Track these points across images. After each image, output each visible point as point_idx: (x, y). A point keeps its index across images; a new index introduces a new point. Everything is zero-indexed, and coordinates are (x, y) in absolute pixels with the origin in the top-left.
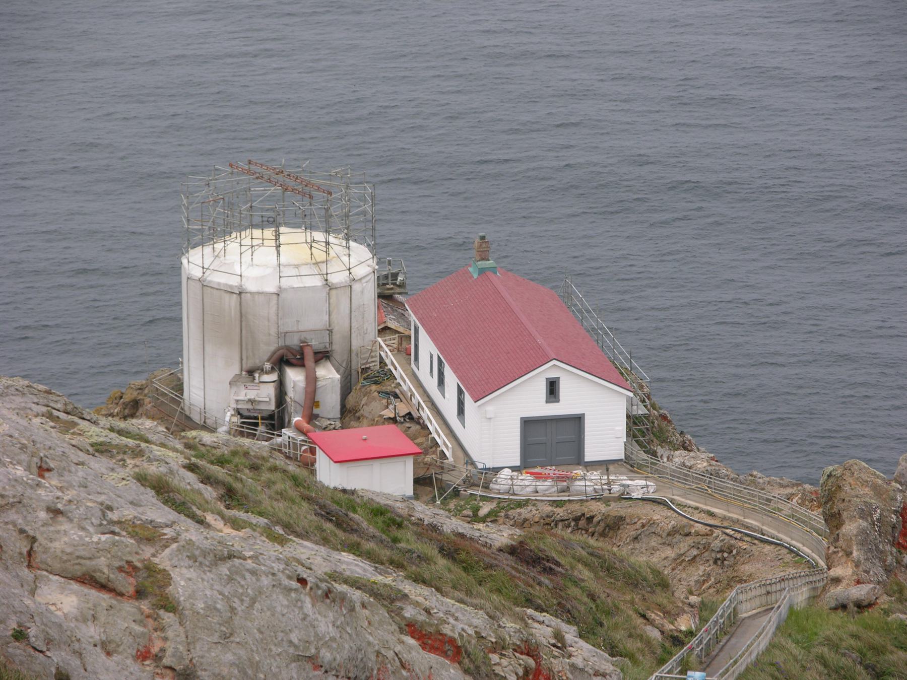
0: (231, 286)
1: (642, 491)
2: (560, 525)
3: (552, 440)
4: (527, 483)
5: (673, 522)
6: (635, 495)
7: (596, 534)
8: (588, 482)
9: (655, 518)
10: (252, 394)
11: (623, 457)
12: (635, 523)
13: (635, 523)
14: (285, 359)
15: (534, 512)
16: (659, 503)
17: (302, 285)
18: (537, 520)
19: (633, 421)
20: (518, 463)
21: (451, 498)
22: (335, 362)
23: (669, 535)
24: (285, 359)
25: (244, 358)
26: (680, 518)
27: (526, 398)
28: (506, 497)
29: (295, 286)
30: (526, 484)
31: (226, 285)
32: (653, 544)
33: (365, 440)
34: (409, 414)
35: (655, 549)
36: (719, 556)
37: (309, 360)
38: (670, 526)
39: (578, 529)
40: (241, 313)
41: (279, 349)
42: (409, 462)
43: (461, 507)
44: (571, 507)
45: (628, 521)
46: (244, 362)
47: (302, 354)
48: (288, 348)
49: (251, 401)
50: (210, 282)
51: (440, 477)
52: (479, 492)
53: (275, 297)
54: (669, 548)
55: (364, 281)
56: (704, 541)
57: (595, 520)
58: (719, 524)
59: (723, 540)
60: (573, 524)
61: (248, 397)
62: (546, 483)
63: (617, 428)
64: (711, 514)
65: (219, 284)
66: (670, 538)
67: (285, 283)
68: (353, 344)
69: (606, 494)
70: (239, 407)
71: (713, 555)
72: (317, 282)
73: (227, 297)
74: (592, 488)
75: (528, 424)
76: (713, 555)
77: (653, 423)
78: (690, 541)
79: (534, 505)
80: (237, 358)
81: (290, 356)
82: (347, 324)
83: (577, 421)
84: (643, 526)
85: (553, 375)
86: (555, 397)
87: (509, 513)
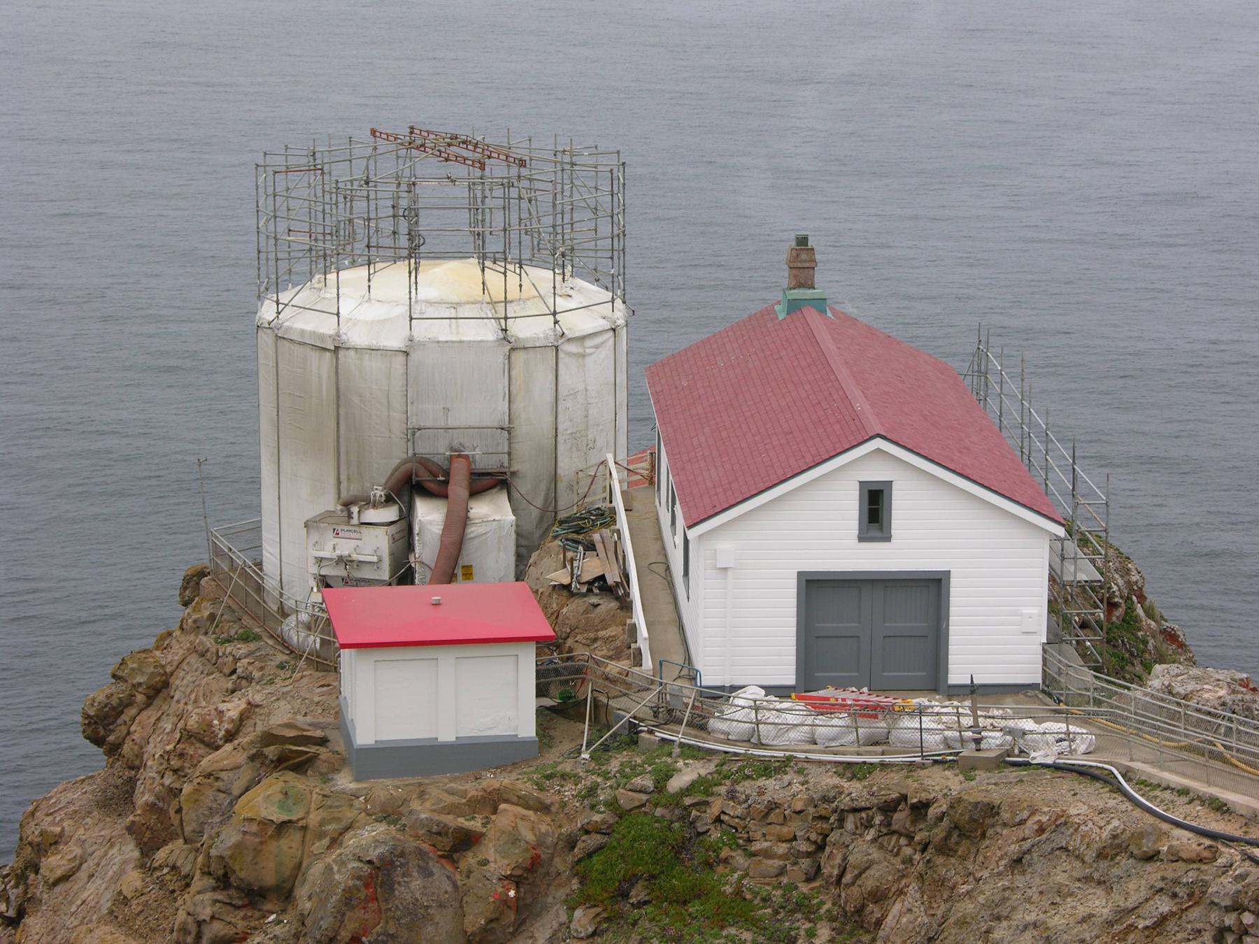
0: (322, 337)
1: (1056, 748)
2: (850, 824)
3: (872, 628)
4: (790, 719)
5: (1115, 823)
6: (1038, 757)
7: (930, 850)
8: (931, 724)
9: (1073, 811)
10: (345, 548)
11: (1038, 679)
12: (1022, 822)
13: (1022, 822)
14: (411, 485)
15: (796, 787)
16: (1095, 778)
17: (454, 339)
18: (799, 806)
19: (1061, 596)
20: (790, 680)
21: (619, 748)
22: (516, 495)
23: (1101, 855)
24: (411, 485)
25: (343, 478)
26: (1138, 813)
27: (812, 526)
28: (741, 751)
29: (441, 339)
30: (791, 726)
31: (313, 333)
32: (1061, 878)
33: (437, 604)
34: (602, 578)
35: (1062, 893)
36: (1230, 920)
37: (458, 488)
38: (1105, 834)
39: (894, 832)
40: (338, 390)
41: (405, 462)
42: (526, 663)
43: (633, 768)
44: (879, 778)
45: (1005, 816)
46: (344, 485)
47: (447, 473)
48: (424, 462)
49: (343, 561)
50: (289, 329)
51: (603, 699)
52: (680, 736)
53: (401, 359)
54: (1100, 891)
55: (589, 343)
56: (1191, 877)
57: (932, 812)
58: (1238, 833)
59: (1242, 877)
60: (878, 820)
61: (338, 552)
62: (835, 722)
63: (1026, 611)
64: (1221, 808)
65: (303, 332)
66: (1103, 864)
67: (423, 331)
68: (560, 464)
69: (968, 751)
70: (323, 572)
71: (1214, 917)
72: (487, 332)
73: (314, 356)
74: (938, 738)
75: (816, 589)
76: (1214, 917)
77: (1145, 643)
78: (1153, 873)
79: (800, 772)
80: (332, 480)
81: (425, 476)
82: (548, 419)
83: (933, 587)
84: (1041, 830)
85: (876, 473)
86: (881, 529)
87: (738, 788)
